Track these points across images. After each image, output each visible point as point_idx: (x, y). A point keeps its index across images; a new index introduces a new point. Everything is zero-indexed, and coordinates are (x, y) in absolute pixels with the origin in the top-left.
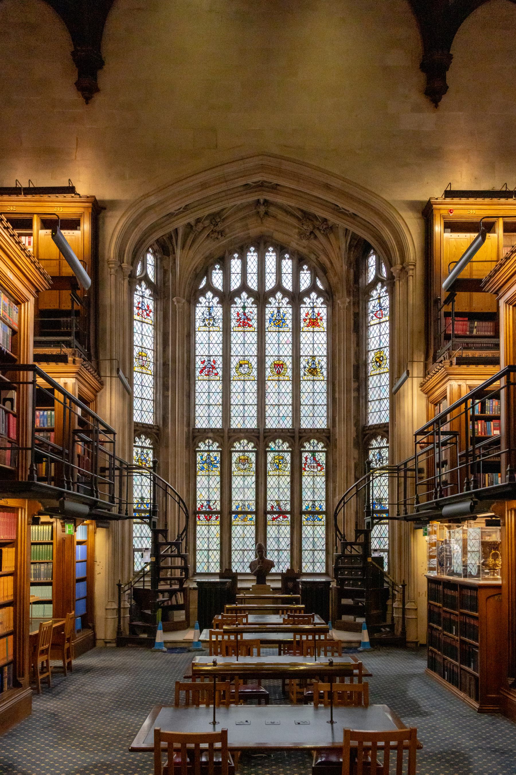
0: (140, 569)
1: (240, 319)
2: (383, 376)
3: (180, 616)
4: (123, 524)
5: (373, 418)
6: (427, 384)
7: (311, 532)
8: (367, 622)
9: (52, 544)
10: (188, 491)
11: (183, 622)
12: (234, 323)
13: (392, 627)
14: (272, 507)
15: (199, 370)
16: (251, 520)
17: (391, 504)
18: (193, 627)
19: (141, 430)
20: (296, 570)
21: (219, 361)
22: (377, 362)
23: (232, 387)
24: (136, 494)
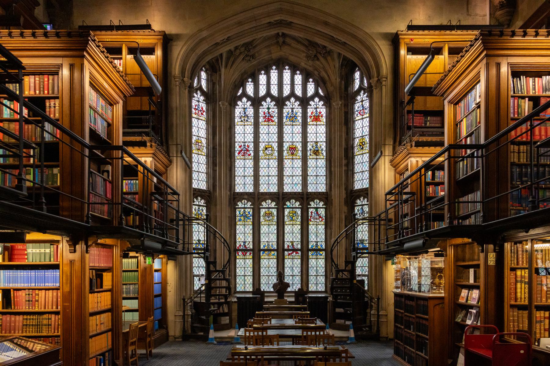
0: (198, 288)
1: (266, 116)
2: (365, 155)
3: (225, 320)
4: (186, 258)
5: (358, 184)
6: (395, 161)
7: (315, 263)
8: (353, 324)
9: (137, 271)
10: (230, 236)
11: (227, 324)
12: (261, 119)
13: (370, 327)
14: (288, 246)
15: (238, 152)
16: (273, 255)
17: (370, 243)
18: (234, 328)
19: (198, 193)
20: (305, 289)
21: (252, 146)
22: (360, 146)
23: (260, 164)
24: (195, 238)
